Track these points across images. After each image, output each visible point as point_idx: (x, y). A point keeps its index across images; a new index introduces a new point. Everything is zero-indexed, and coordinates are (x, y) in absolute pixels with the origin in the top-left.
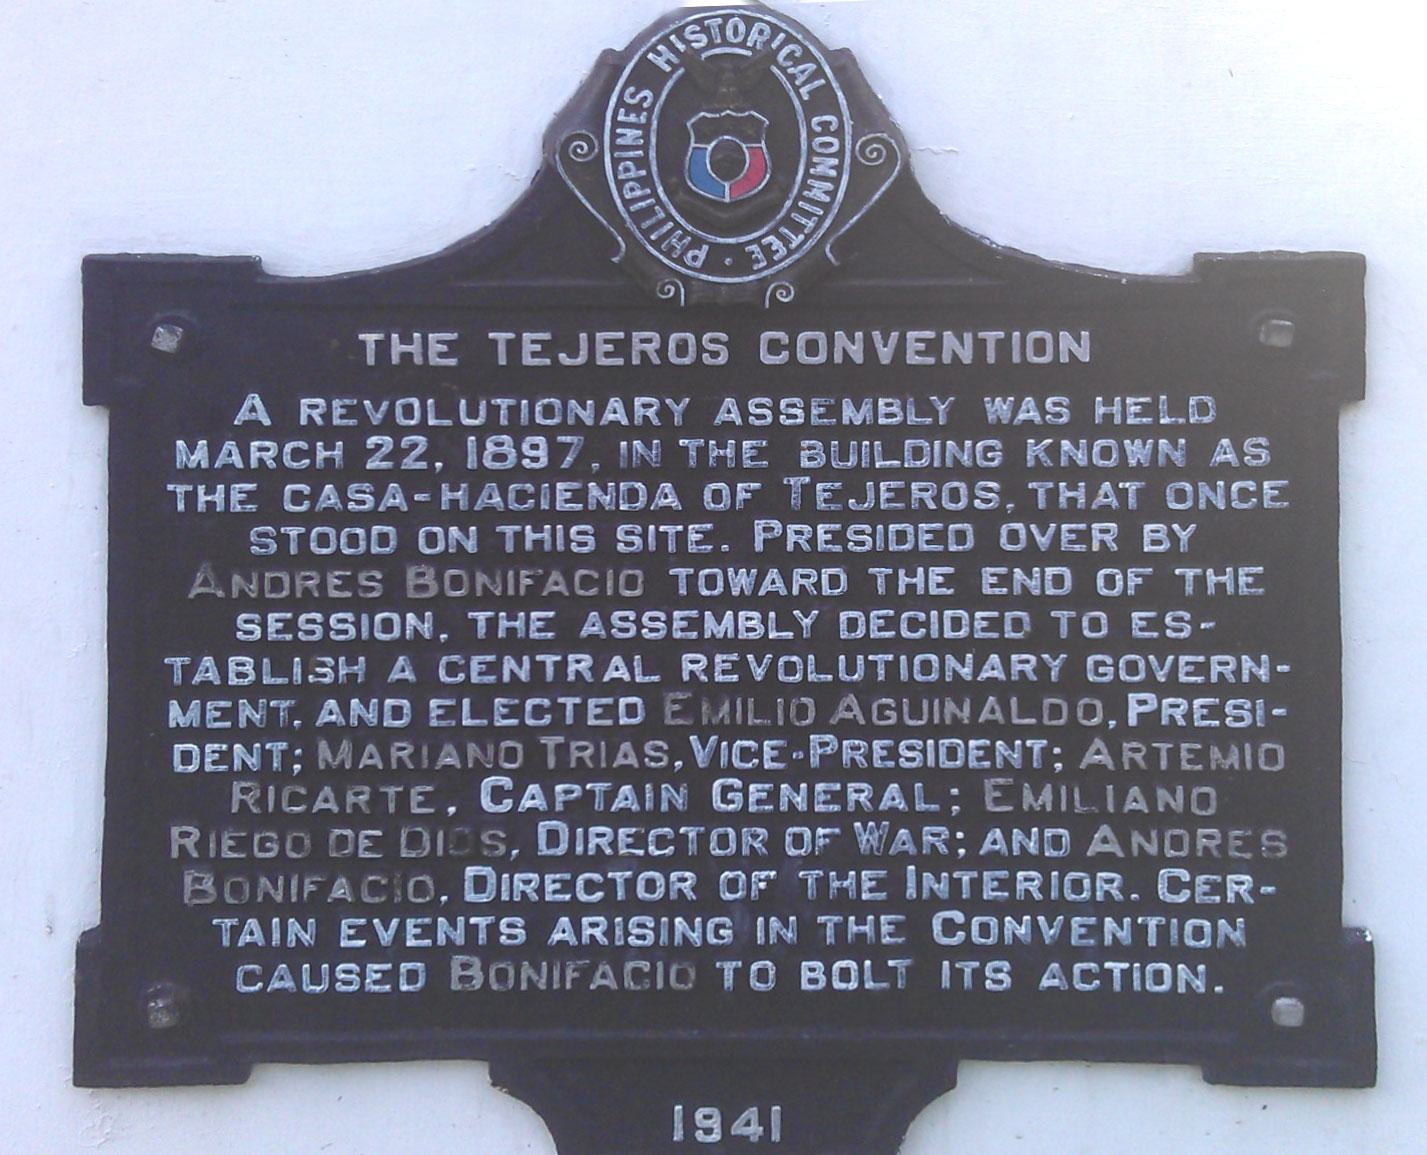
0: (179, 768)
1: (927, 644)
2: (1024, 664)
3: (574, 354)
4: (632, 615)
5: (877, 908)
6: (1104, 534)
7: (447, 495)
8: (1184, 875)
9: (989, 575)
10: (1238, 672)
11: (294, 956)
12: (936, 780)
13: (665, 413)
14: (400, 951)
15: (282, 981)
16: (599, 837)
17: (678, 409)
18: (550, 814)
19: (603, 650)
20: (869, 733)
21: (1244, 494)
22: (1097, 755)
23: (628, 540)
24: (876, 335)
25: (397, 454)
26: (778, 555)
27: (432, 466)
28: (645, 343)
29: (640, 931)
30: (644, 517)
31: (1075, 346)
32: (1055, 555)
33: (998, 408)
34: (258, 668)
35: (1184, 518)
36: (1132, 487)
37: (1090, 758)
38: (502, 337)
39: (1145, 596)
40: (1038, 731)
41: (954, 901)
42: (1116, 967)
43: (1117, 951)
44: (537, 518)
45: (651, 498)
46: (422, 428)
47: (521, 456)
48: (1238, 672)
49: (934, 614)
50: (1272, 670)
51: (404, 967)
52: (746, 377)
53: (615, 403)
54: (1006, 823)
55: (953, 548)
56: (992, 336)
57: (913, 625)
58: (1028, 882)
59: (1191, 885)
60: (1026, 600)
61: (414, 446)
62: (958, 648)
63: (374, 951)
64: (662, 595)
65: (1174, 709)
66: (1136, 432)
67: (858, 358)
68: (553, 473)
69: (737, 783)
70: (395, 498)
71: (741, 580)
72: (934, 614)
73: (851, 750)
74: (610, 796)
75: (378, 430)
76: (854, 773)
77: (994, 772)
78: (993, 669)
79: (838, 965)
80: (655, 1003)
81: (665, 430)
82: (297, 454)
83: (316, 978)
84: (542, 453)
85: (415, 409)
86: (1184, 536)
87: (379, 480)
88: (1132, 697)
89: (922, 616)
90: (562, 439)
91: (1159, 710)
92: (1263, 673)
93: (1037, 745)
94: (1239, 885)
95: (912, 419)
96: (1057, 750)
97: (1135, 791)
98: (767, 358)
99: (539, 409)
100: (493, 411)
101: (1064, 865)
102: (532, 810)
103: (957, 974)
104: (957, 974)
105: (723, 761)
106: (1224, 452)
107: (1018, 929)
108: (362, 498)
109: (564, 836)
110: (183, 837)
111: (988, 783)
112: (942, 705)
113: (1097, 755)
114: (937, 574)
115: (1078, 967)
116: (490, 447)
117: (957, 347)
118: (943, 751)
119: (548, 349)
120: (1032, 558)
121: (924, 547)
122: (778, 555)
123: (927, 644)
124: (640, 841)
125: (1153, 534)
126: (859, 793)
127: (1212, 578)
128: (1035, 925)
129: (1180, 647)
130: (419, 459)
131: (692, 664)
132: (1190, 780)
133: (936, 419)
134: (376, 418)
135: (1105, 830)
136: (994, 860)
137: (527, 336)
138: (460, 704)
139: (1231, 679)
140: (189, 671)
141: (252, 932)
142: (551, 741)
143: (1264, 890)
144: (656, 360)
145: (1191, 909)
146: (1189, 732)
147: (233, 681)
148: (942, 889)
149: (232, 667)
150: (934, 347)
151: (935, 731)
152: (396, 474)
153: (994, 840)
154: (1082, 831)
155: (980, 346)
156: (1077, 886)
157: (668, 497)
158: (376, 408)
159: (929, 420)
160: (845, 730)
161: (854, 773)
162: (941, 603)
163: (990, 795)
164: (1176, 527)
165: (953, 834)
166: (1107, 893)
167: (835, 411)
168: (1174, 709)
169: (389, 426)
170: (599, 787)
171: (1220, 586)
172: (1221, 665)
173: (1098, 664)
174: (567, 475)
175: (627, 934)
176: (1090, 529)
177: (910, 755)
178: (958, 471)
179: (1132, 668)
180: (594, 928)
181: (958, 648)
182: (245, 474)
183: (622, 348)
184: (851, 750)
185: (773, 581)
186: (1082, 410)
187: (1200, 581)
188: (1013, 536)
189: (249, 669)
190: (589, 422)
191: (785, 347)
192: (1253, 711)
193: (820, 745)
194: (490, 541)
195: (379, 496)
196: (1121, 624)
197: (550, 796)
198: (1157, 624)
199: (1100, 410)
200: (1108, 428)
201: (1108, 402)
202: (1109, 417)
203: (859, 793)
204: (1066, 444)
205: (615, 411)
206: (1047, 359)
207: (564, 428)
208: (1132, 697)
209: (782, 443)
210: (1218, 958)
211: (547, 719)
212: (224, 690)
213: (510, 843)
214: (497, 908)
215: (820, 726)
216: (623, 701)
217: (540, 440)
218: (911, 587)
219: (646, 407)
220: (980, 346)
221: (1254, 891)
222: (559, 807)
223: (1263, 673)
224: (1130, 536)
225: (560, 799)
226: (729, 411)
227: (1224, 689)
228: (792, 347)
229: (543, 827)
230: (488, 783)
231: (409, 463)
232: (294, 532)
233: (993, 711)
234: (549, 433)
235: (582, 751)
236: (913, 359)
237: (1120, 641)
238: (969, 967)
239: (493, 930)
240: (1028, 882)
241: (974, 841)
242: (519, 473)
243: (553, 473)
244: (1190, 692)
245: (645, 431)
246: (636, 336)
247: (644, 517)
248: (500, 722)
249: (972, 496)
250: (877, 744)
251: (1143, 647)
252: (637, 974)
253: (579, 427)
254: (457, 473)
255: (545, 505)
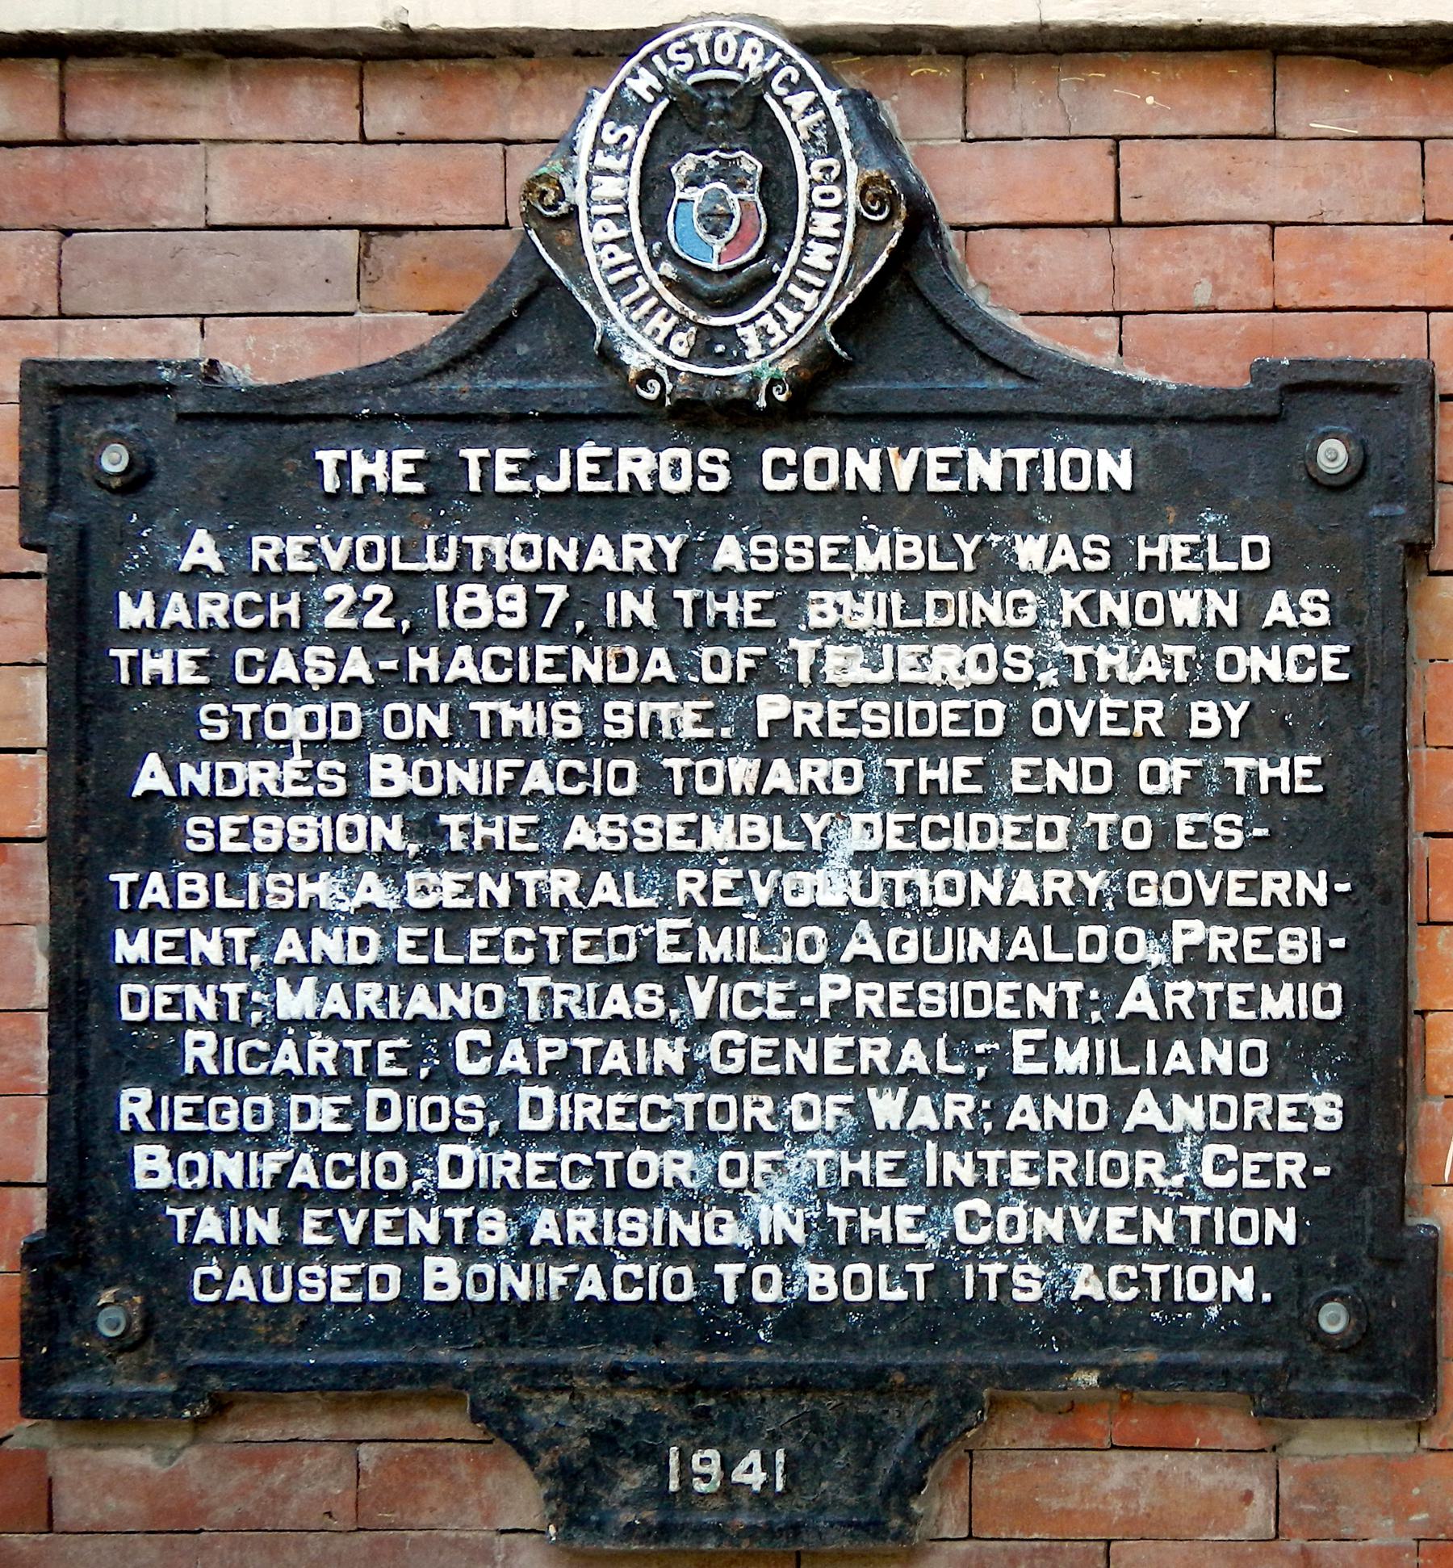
0: (127, 1015)
1: (948, 857)
2: (1058, 884)
3: (555, 475)
4: (622, 819)
5: (891, 1197)
6: (1151, 715)
7: (415, 661)
8: (1231, 1152)
9: (1019, 767)
10: (1292, 893)
11: (255, 1253)
12: (960, 1031)
13: (658, 554)
14: (366, 1249)
15: (242, 1285)
16: (585, 1109)
17: (671, 549)
18: (533, 1078)
19: (588, 862)
20: (886, 972)
21: (1303, 662)
22: (1138, 999)
23: (620, 718)
24: (893, 452)
25: (359, 607)
26: (783, 741)
27: (398, 624)
28: (637, 463)
29: (635, 1226)
30: (635, 690)
31: (1116, 469)
32: (1093, 742)
33: (1029, 551)
34: (211, 887)
35: (1230, 691)
36: (1179, 652)
37: (1129, 1006)
38: (472, 455)
39: (1190, 796)
40: (1073, 969)
41: (980, 1188)
42: (1155, 1271)
43: (1159, 1251)
44: (514, 691)
45: (642, 664)
46: (385, 574)
47: (496, 611)
48: (1292, 893)
49: (959, 817)
50: (1331, 892)
51: (375, 1270)
52: (742, 508)
53: (600, 541)
54: (1036, 1085)
55: (980, 732)
56: (1023, 455)
57: (936, 831)
58: (1062, 1164)
59: (1238, 1165)
60: (1059, 801)
61: (377, 598)
62: (985, 861)
63: (340, 1251)
64: (656, 794)
65: (1220, 941)
66: (1184, 579)
67: (874, 484)
68: (531, 632)
69: (739, 1037)
70: (357, 665)
71: (742, 772)
72: (959, 817)
73: (868, 998)
74: (598, 1053)
75: (340, 576)
76: (870, 1025)
77: (1023, 1022)
78: (1024, 890)
79: (850, 1270)
80: (650, 1320)
81: (657, 579)
82: (249, 608)
83: (277, 1287)
84: (520, 606)
85: (379, 546)
86: (1235, 716)
87: (340, 640)
88: (1178, 925)
89: (945, 822)
90: (541, 589)
91: (1205, 945)
92: (1321, 898)
93: (1072, 988)
94: (1291, 1166)
95: (935, 565)
96: (1094, 994)
97: (1179, 1047)
98: (770, 483)
99: (510, 548)
100: (465, 550)
101: (1097, 1140)
102: (512, 1073)
103: (981, 1280)
104: (981, 1280)
105: (724, 1014)
106: (1279, 609)
107: (1048, 1224)
108: (319, 665)
109: (549, 1106)
110: (134, 1103)
111: (1019, 1035)
112: (967, 935)
113: (1138, 999)
114: (962, 764)
115: (1114, 1270)
116: (462, 602)
117: (985, 470)
118: (967, 996)
119: (526, 469)
120: (1063, 745)
121: (947, 732)
122: (783, 741)
123: (948, 857)
124: (631, 1110)
125: (1205, 717)
126: (874, 1051)
127: (1266, 773)
128: (1068, 1222)
129: (1228, 858)
130: (383, 615)
131: (687, 884)
132: (1241, 1028)
133: (961, 566)
134: (336, 560)
135: (1145, 1096)
136: (1022, 1137)
137: (502, 454)
138: (432, 934)
139: (1286, 903)
140: (136, 889)
141: (210, 1227)
142: (533, 984)
143: (1319, 1171)
144: (646, 485)
145: (1237, 1195)
146: (1242, 970)
147: (184, 903)
148: (968, 1177)
149: (183, 888)
150: (957, 467)
151: (958, 971)
152: (360, 634)
153: (1022, 1112)
154: (1122, 1093)
155: (1010, 463)
156: (1114, 1168)
157: (660, 664)
158: (335, 546)
159: (952, 566)
160: (861, 968)
161: (870, 1025)
162: (968, 803)
163: (1020, 1051)
164: (1226, 705)
165: (978, 1105)
166: (1148, 1178)
167: (845, 552)
168: (1220, 941)
169: (349, 572)
170: (587, 1044)
171: (1274, 782)
172: (1275, 884)
173: (1140, 882)
174: (551, 635)
175: (616, 1229)
176: (1132, 705)
177: (936, 999)
178: (985, 633)
179: (1177, 887)
180: (581, 1222)
181: (985, 861)
182: (194, 634)
183: (607, 467)
184: (868, 998)
185: (779, 777)
186: (1120, 551)
187: (1253, 775)
188: (1047, 715)
189: (200, 888)
190: (572, 566)
191: (793, 469)
192: (1309, 943)
193: (832, 988)
194: (463, 719)
195: (339, 662)
196: (1165, 832)
197: (531, 1054)
198: (1202, 831)
199: (1144, 552)
200: (1156, 576)
201: (1152, 542)
202: (1152, 560)
203: (874, 1051)
204: (1106, 598)
205: (601, 553)
206: (1084, 485)
207: (542, 574)
208: (1178, 925)
209: (789, 590)
210: (1267, 1258)
211: (528, 956)
212: (175, 915)
213: (488, 1112)
214: (477, 1195)
215: (834, 962)
216: (613, 932)
217: (519, 590)
218: (933, 784)
219: (637, 550)
220: (1010, 463)
221: (1306, 1173)
222: (542, 1071)
223: (1321, 898)
224: (1177, 720)
225: (544, 1057)
226: (729, 553)
227: (1277, 915)
228: (798, 468)
229: (526, 1092)
230: (463, 1037)
231: (373, 619)
232: (246, 710)
233: (1023, 944)
234: (529, 579)
235: (568, 997)
236: (934, 485)
237: (1162, 854)
238: (993, 1270)
239: (471, 1223)
240: (1062, 1164)
241: (998, 1114)
242: (493, 632)
243: (531, 632)
244: (1241, 917)
245: (635, 579)
246: (625, 453)
247: (635, 690)
248: (476, 959)
249: (1001, 664)
250: (895, 986)
251: (1189, 859)
252: (628, 1281)
253: (560, 572)
254: (421, 634)
255: (524, 676)
